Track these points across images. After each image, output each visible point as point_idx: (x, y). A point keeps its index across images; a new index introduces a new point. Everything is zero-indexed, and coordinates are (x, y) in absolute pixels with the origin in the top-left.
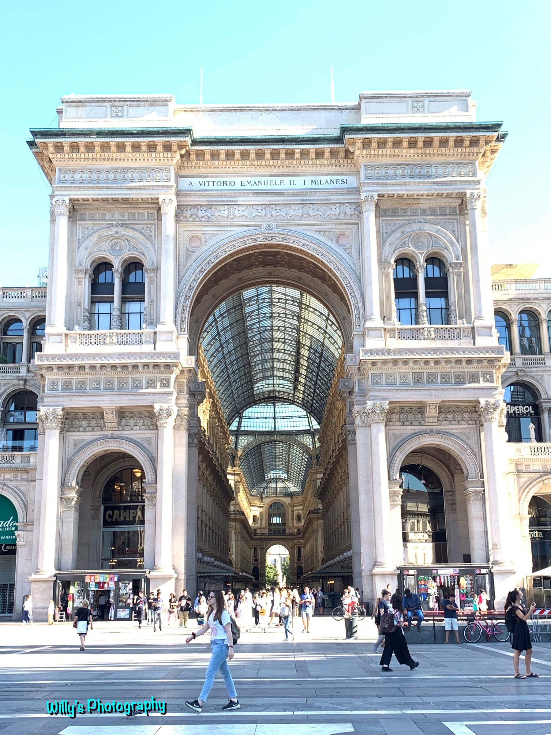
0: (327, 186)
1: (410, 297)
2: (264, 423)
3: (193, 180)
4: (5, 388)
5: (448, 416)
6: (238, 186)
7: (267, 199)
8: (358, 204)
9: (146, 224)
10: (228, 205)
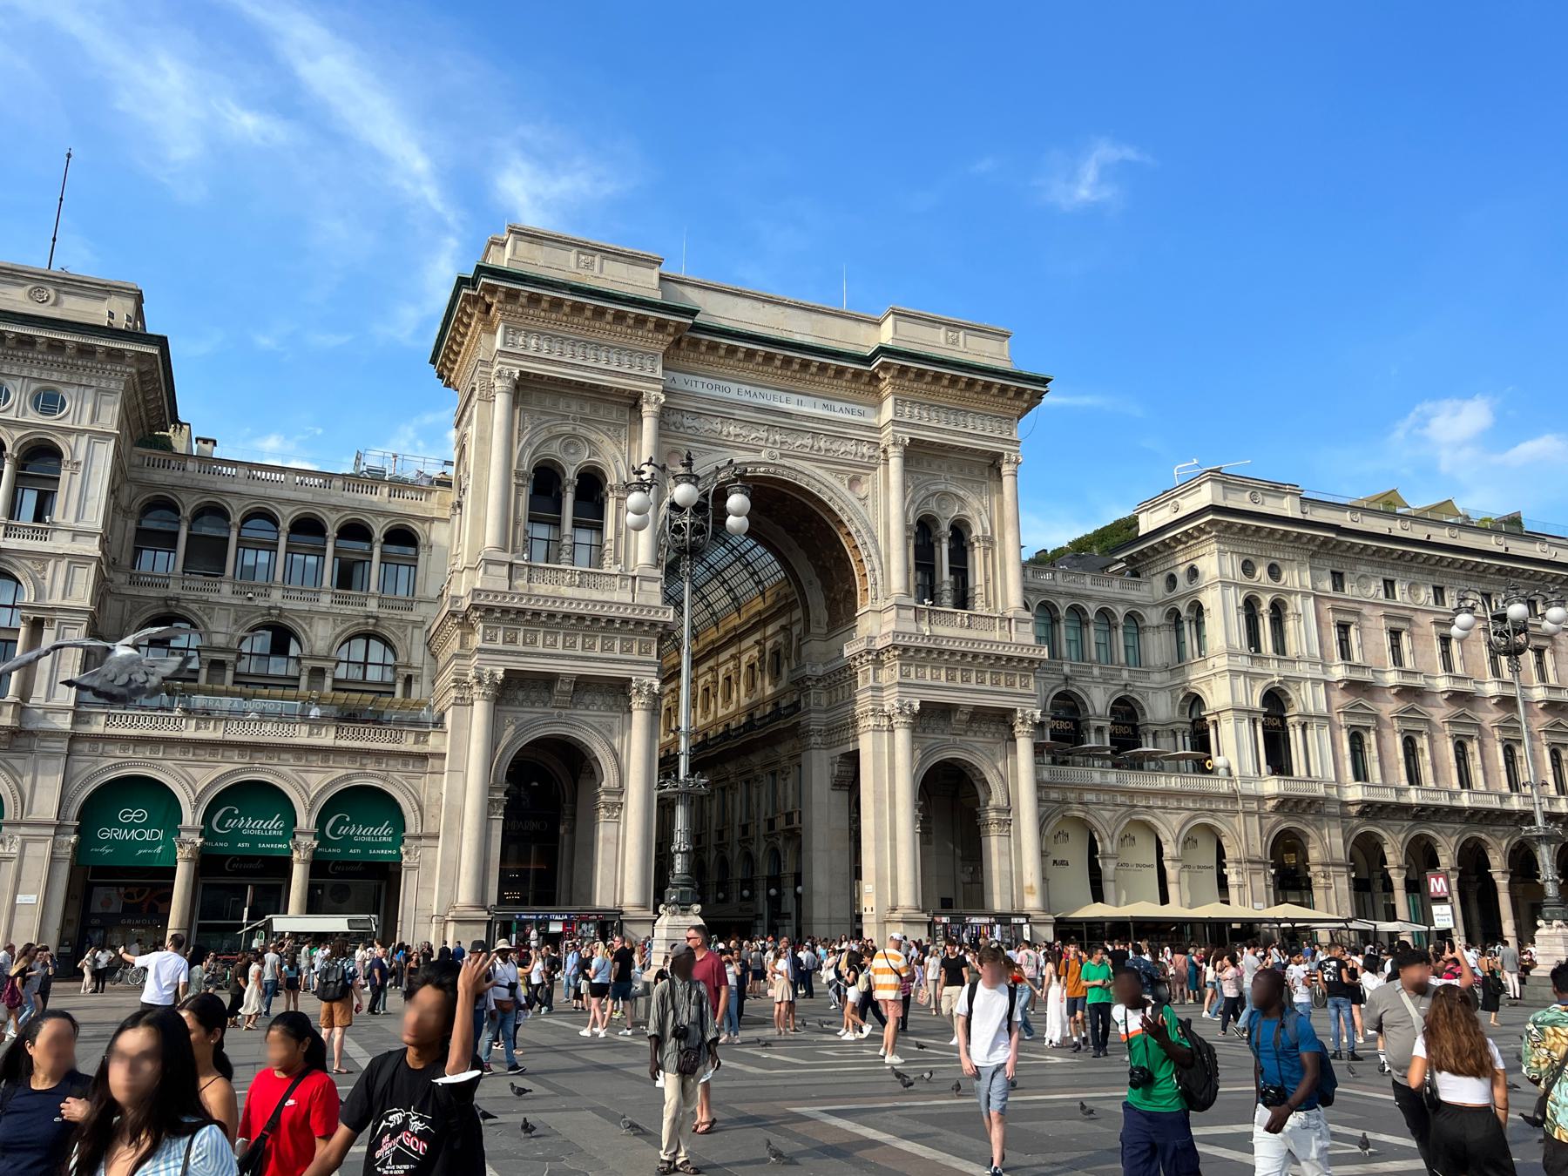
4: (345, 626)
6: (733, 395)
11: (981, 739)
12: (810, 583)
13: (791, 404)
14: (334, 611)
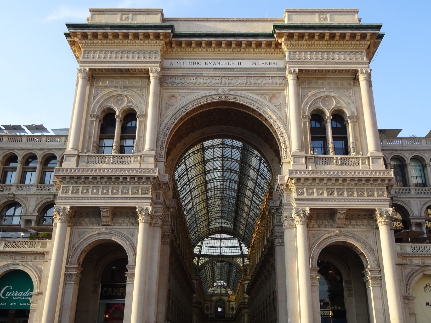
0: (263, 66)
1: (321, 140)
2: (215, 250)
3: (173, 61)
5: (352, 221)
6: (203, 65)
7: (223, 73)
8: (284, 78)
9: (140, 87)
10: (196, 76)
11: (358, 229)
12: (273, 160)
13: (236, 64)
14: (37, 193)
